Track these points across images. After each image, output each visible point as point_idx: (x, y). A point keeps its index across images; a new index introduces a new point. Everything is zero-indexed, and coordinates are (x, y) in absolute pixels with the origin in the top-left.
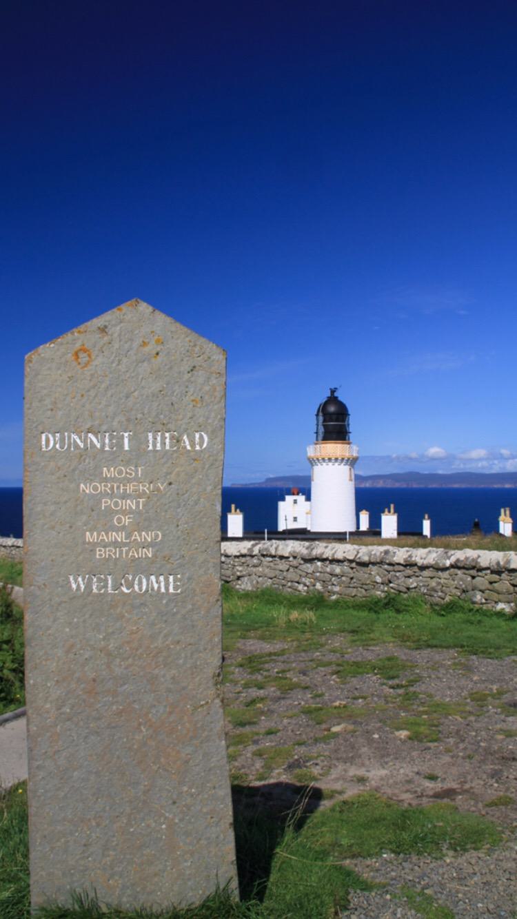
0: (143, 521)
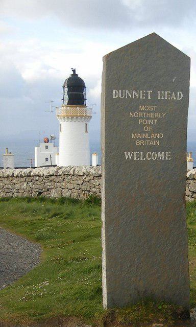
0: (156, 129)
